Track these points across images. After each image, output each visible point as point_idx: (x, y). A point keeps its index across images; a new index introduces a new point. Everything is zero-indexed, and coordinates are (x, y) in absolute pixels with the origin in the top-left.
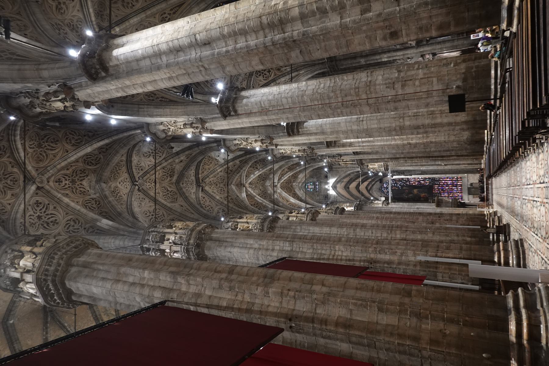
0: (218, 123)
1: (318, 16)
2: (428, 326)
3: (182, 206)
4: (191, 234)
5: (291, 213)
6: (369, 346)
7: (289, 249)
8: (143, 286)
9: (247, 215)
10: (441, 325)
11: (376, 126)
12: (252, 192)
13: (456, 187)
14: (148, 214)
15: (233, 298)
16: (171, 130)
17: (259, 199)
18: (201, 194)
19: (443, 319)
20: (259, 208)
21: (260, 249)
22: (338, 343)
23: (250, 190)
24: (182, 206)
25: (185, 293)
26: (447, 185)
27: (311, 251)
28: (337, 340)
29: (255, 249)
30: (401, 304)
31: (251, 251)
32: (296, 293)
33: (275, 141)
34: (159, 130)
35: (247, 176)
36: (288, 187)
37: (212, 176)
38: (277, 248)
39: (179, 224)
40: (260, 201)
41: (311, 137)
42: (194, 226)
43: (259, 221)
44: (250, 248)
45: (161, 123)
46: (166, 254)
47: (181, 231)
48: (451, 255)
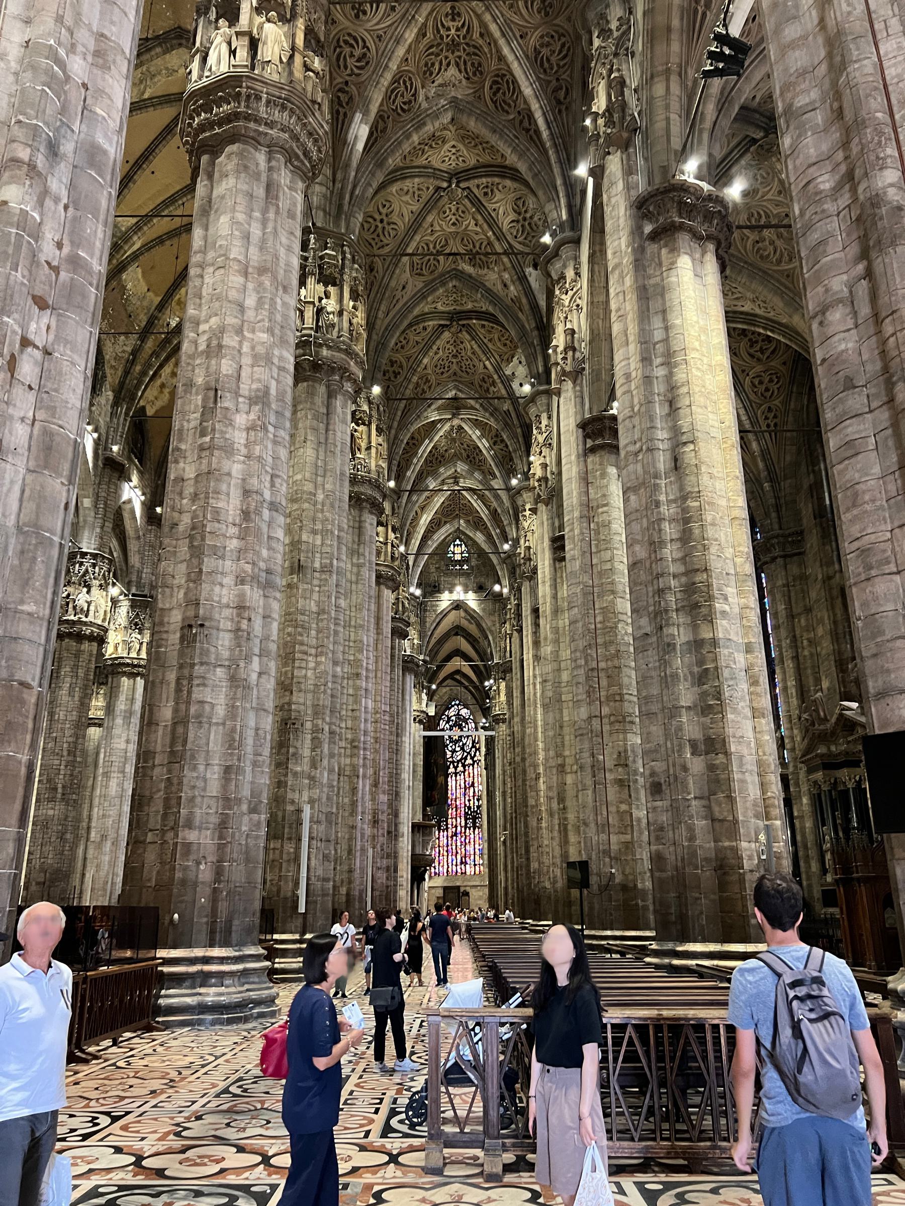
0: (572, 410)
1: (696, 669)
3: (404, 288)
4: (340, 350)
5: (394, 530)
6: (172, 753)
9: (385, 445)
11: (566, 719)
12: (441, 433)
13: (462, 863)
14: (384, 211)
16: (564, 297)
17: (426, 447)
19: (220, 861)
20: (399, 465)
22: (171, 703)
23: (447, 427)
24: (404, 288)
25: (231, 424)
28: (177, 703)
30: (239, 801)
33: (542, 507)
34: (565, 266)
35: (476, 423)
36: (455, 508)
37: (475, 346)
39: (360, 318)
40: (420, 452)
41: (548, 584)
42: (357, 355)
43: (374, 475)
45: (578, 274)
47: (346, 325)
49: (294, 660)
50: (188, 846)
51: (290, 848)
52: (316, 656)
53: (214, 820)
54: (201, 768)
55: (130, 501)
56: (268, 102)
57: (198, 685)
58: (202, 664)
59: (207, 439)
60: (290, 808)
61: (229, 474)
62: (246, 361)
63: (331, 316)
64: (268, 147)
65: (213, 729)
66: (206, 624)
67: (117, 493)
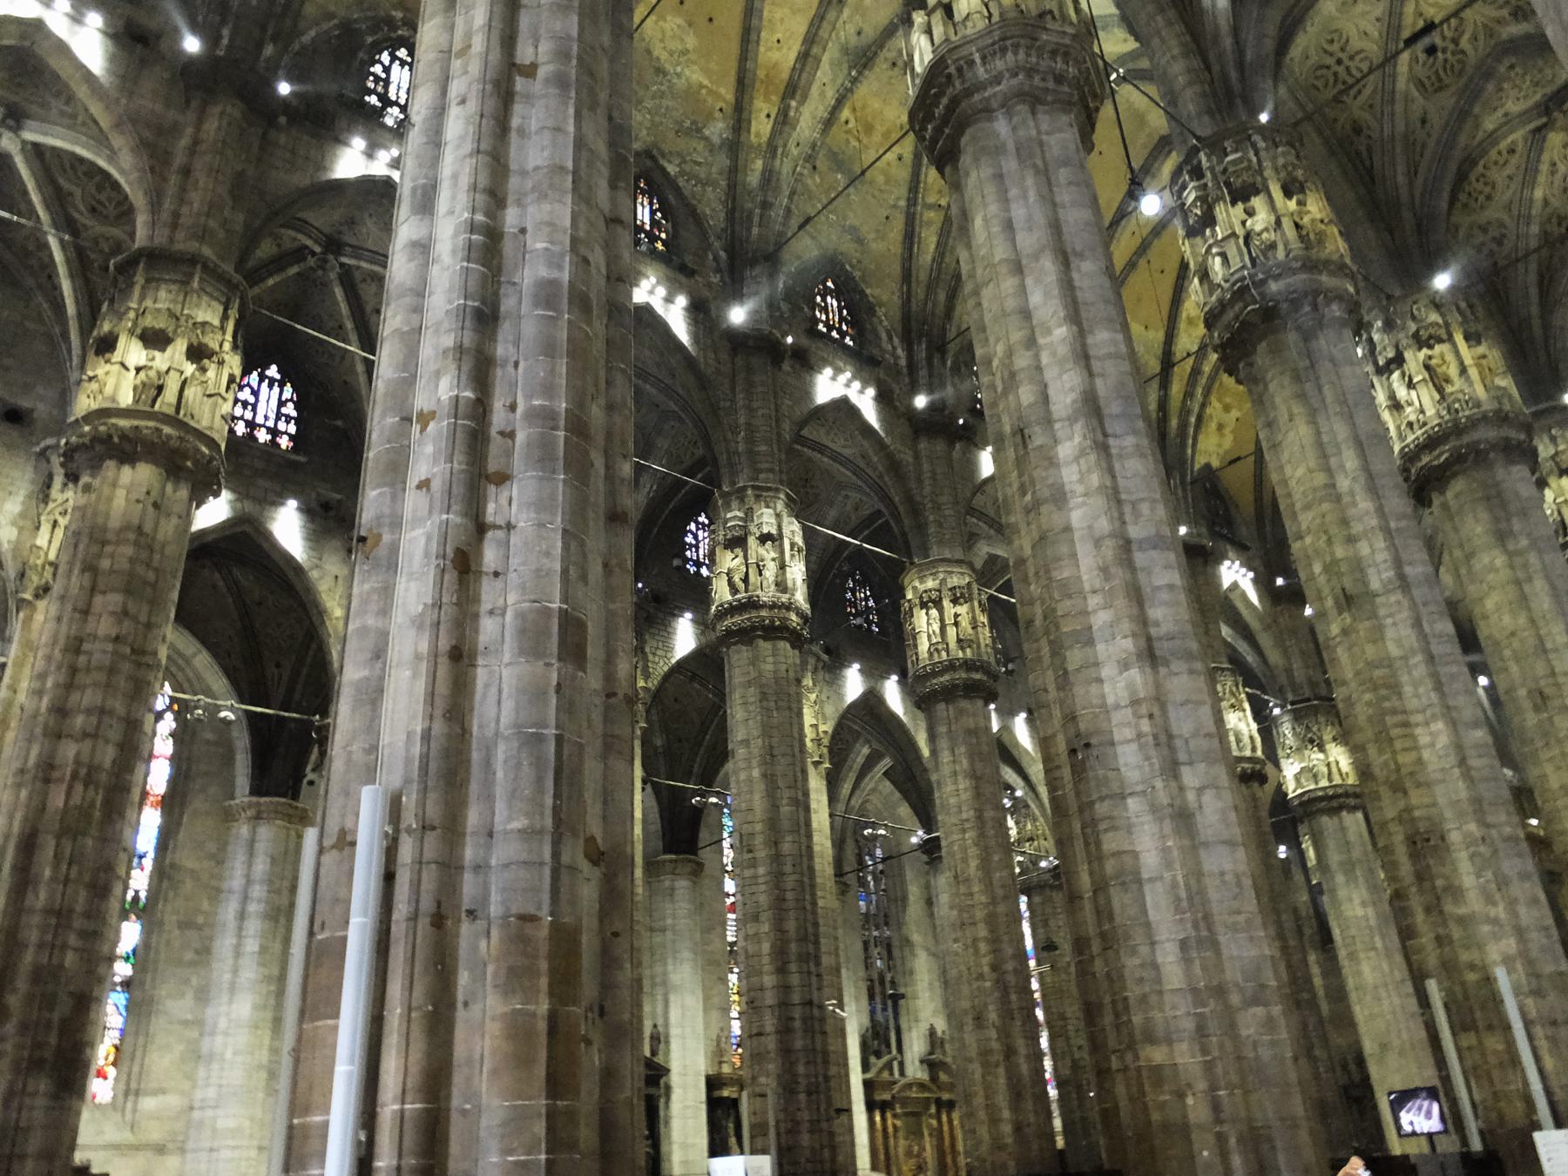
2: (1185, 1056)
3: (1424, 121)
4: (1294, 272)
7: (1375, 584)
8: (1031, 342)
10: (1201, 1085)
14: (1335, 47)
15: (1087, 587)
18: (1518, 136)
19: (1213, 1088)
21: (1338, 498)
24: (1424, 121)
25: (1052, 462)
27: (1394, 650)
29: (1334, 486)
31: (1320, 479)
32: (1151, 738)
38: (1364, 549)
43: (1488, 406)
44: (1328, 470)
46: (1208, 232)
48: (1549, 1063)
49: (1391, 740)
50: (1157, 1070)
51: (1494, 1043)
52: (1427, 724)
53: (1188, 1025)
54: (1144, 950)
55: (1235, 586)
56: (984, 58)
57: (1106, 830)
58: (1102, 799)
59: (1028, 497)
60: (1472, 977)
61: (1068, 529)
62: (1050, 374)
63: (1265, 235)
64: (1003, 106)
65: (1147, 888)
66: (1093, 741)
67: (1214, 580)
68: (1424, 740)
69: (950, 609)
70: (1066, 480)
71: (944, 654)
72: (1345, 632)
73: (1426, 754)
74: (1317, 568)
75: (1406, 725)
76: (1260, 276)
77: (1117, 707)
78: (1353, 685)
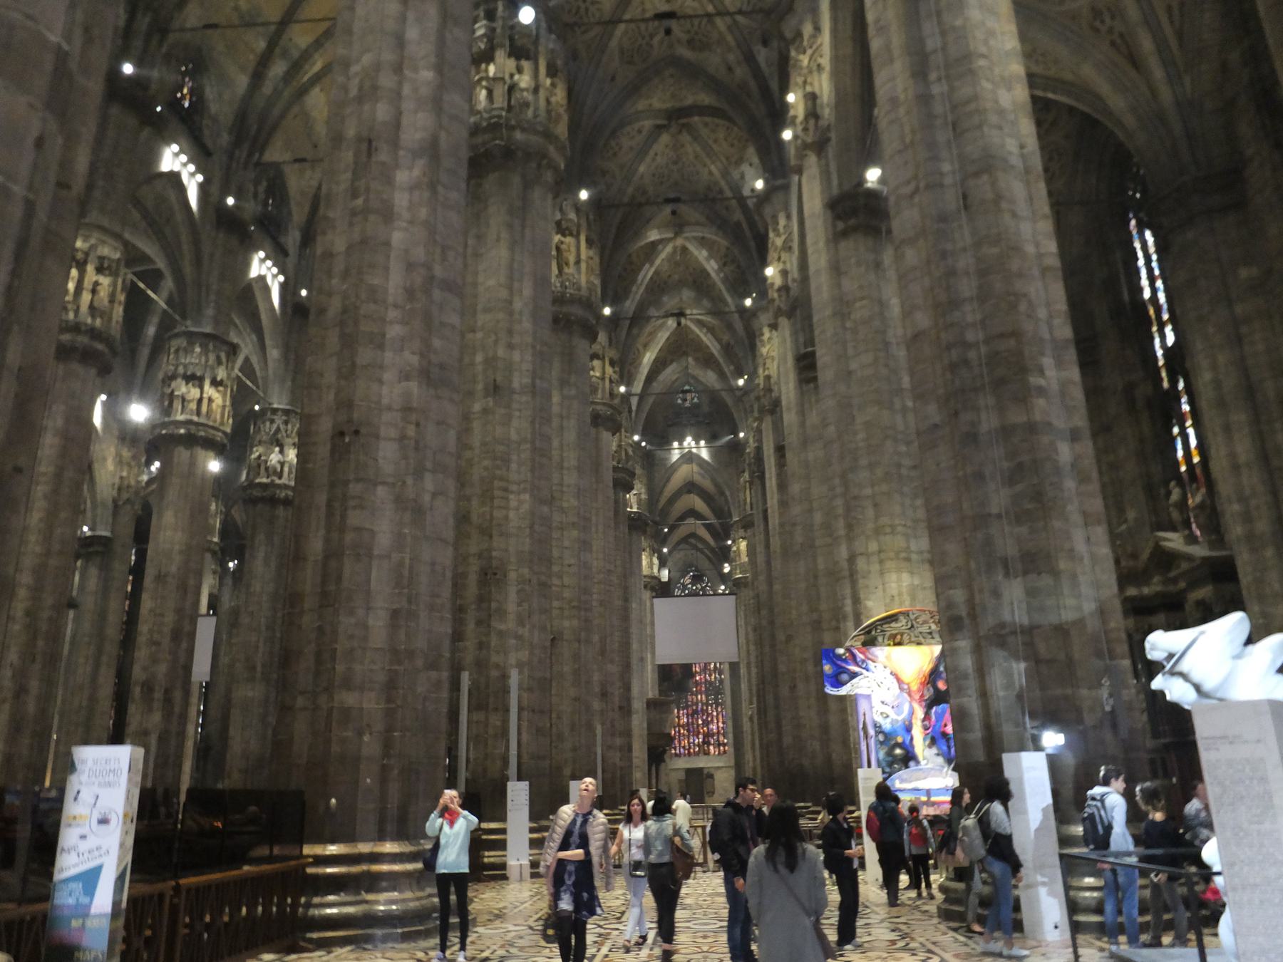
0: (817, 189)
1: (1006, 465)
2: (371, 703)
3: (613, 79)
4: (536, 132)
5: (612, 364)
6: (324, 594)
7: (516, 385)
8: (398, 69)
9: (597, 260)
10: (379, 727)
11: (821, 566)
12: (663, 255)
13: (704, 742)
15: (391, 299)
16: (801, 57)
17: (647, 273)
18: (647, 124)
19: (389, 729)
21: (511, 314)
22: (322, 532)
23: (669, 249)
25: (389, 181)
26: (706, 723)
27: (514, 436)
28: (328, 530)
29: (511, 303)
30: (411, 654)
31: (504, 294)
32: (413, 442)
33: (784, 322)
34: (801, 22)
35: (702, 242)
36: (680, 346)
37: (698, 149)
38: (516, 356)
39: (560, 96)
40: (640, 278)
41: (794, 412)
42: (557, 138)
43: (584, 293)
44: (510, 289)
45: (817, 29)
46: (483, 66)
47: (542, 103)
48: (525, 737)
49: (492, 499)
50: (346, 713)
52: (519, 494)
53: (381, 678)
57: (355, 508)
58: (358, 480)
59: (360, 201)
60: (494, 673)
61: (387, 244)
62: (407, 105)
63: (525, 94)
65: (375, 563)
66: (363, 431)
68: (513, 504)
69: (91, 275)
70: (397, 202)
71: (71, 315)
72: (485, 411)
73: (512, 514)
74: (479, 358)
75: (506, 490)
76: (513, 122)
77: (390, 408)
78: (477, 451)
